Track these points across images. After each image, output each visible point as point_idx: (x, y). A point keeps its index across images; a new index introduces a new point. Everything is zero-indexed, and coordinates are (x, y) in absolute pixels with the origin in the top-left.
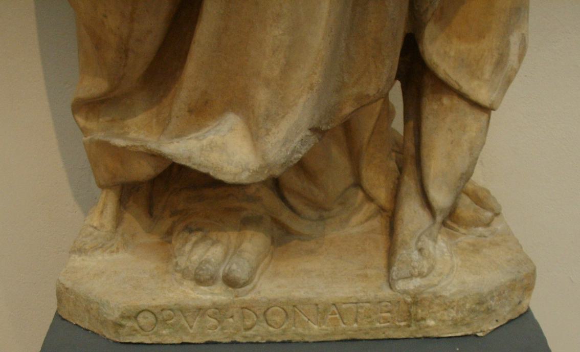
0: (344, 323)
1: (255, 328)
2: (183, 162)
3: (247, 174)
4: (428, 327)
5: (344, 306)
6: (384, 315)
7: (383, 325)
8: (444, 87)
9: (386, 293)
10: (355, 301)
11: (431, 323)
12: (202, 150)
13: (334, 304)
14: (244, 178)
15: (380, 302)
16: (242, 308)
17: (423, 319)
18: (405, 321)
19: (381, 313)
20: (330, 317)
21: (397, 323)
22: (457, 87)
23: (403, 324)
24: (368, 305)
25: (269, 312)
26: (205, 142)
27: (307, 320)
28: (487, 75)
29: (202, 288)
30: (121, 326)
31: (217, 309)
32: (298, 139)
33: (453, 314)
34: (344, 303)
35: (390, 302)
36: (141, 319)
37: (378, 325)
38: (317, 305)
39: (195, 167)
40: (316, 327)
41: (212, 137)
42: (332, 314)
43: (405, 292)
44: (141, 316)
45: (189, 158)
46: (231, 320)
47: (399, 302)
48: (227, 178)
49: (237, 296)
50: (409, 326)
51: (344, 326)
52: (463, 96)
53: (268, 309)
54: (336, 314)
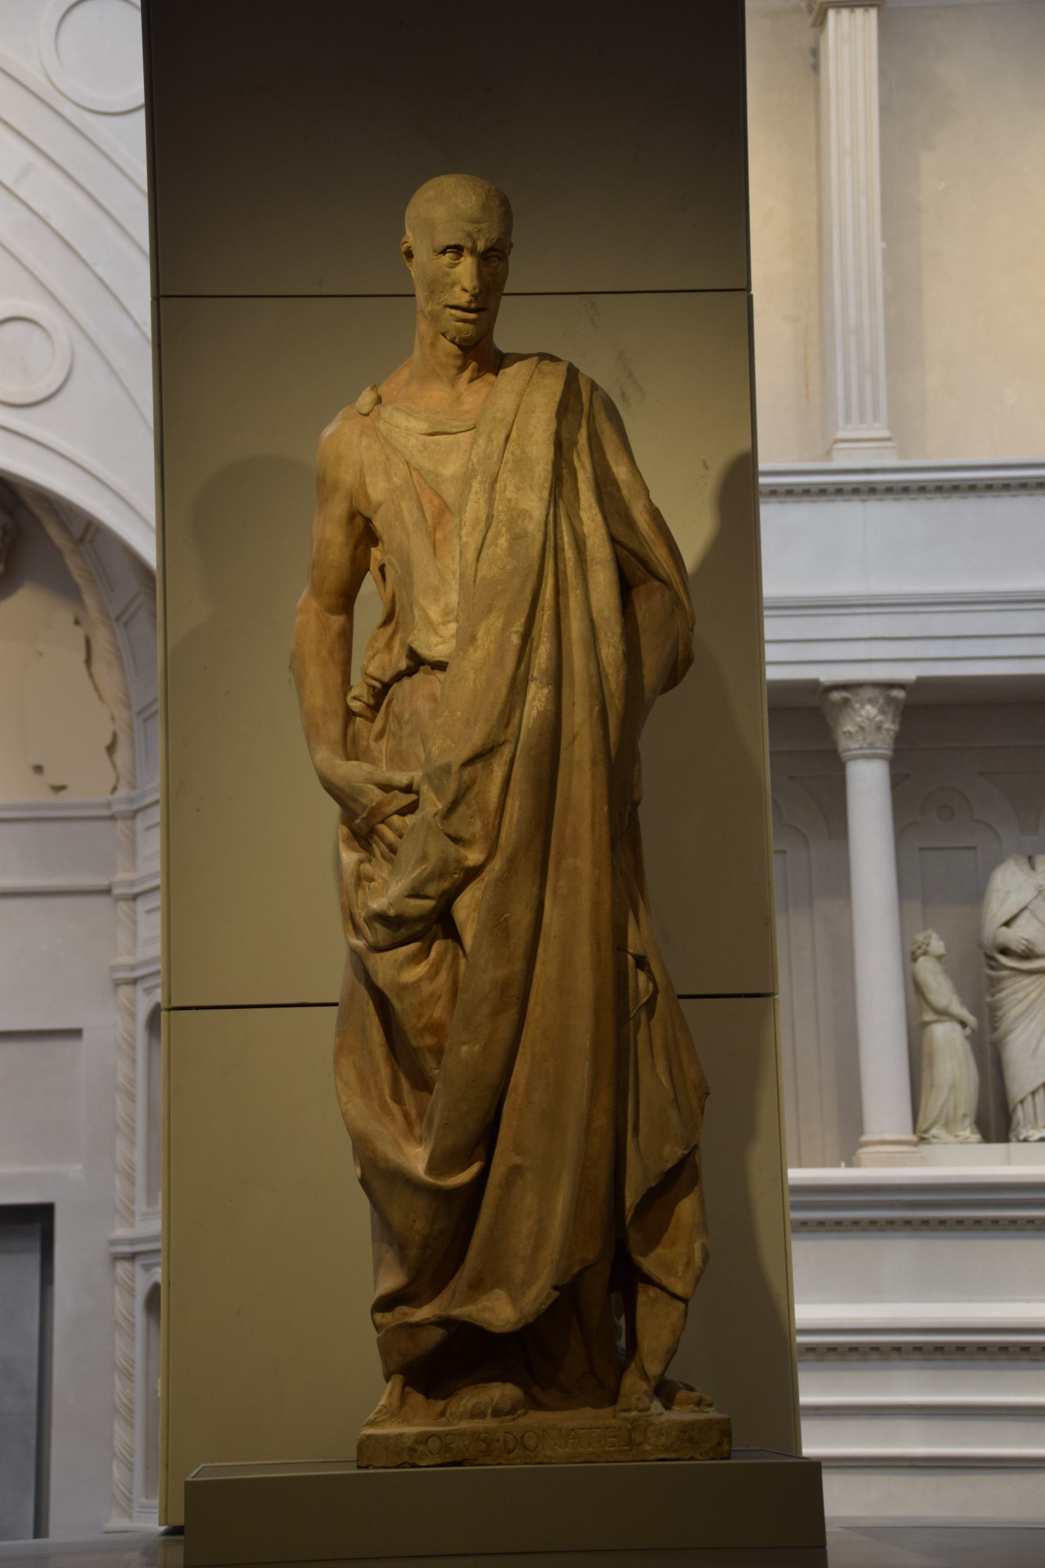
0: (582, 1447)
1: (515, 1452)
2: (467, 1319)
3: (509, 1325)
4: (645, 1451)
5: (581, 1431)
6: (611, 1439)
7: (611, 1449)
8: (649, 1281)
9: (613, 1422)
10: (587, 1426)
11: (648, 1448)
12: (478, 1310)
13: (573, 1430)
14: (508, 1328)
15: (607, 1428)
16: (507, 1433)
17: (641, 1444)
18: (626, 1446)
19: (609, 1438)
20: (571, 1441)
21: (622, 1448)
22: (658, 1281)
23: (626, 1448)
24: (598, 1431)
25: (526, 1436)
26: (480, 1306)
27: (554, 1443)
28: (680, 1273)
29: (476, 1420)
30: (415, 1450)
31: (486, 1433)
32: (544, 1295)
33: (663, 1439)
34: (581, 1429)
35: (614, 1428)
36: (430, 1442)
37: (607, 1449)
38: (560, 1430)
39: (474, 1322)
40: (561, 1450)
41: (484, 1303)
42: (571, 1439)
43: (626, 1419)
44: (430, 1441)
45: (470, 1316)
46: (497, 1444)
47: (621, 1428)
48: (497, 1330)
49: (502, 1422)
50: (631, 1450)
51: (582, 1449)
52: (663, 1289)
53: (525, 1433)
54: (575, 1439)
